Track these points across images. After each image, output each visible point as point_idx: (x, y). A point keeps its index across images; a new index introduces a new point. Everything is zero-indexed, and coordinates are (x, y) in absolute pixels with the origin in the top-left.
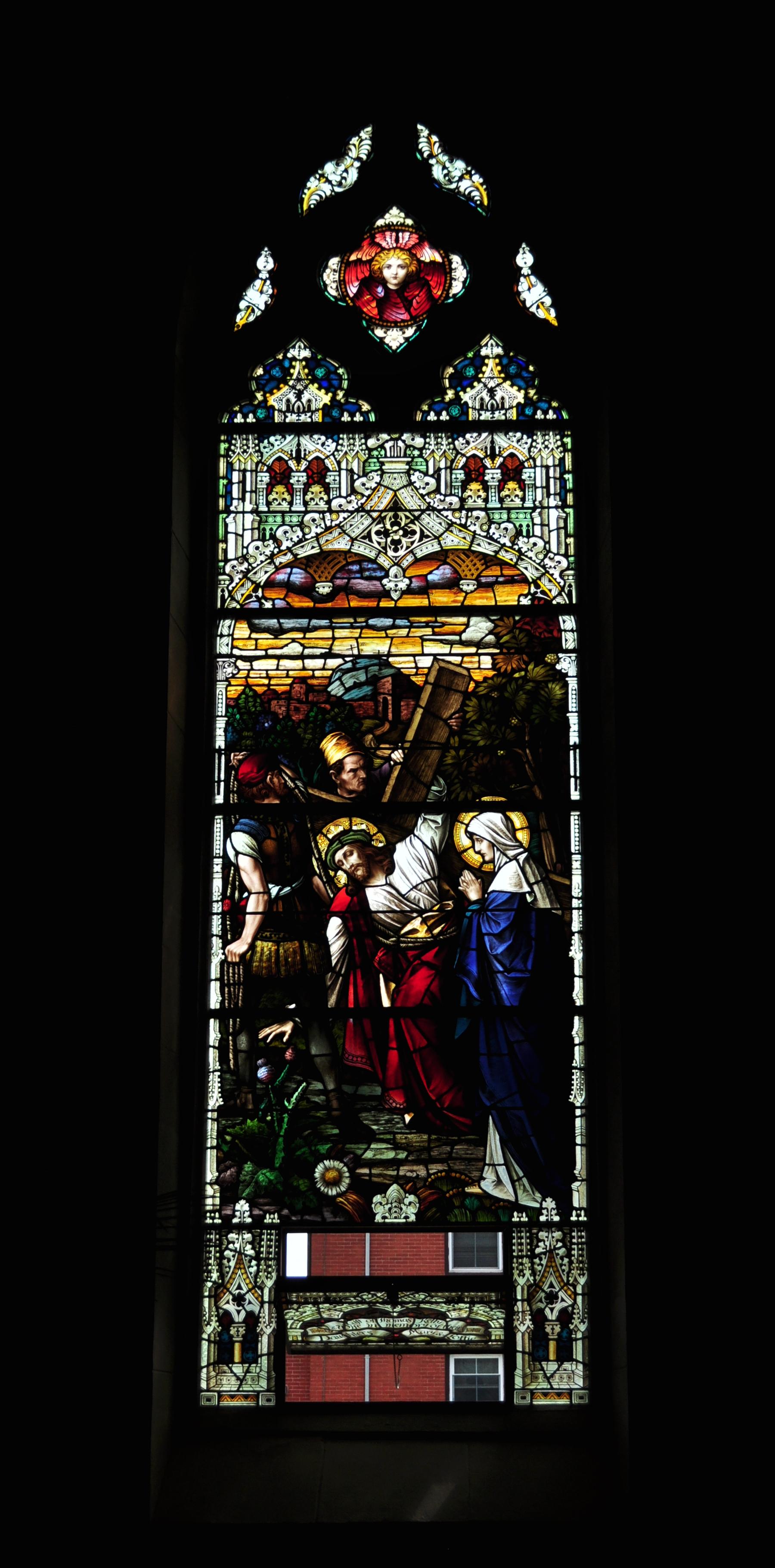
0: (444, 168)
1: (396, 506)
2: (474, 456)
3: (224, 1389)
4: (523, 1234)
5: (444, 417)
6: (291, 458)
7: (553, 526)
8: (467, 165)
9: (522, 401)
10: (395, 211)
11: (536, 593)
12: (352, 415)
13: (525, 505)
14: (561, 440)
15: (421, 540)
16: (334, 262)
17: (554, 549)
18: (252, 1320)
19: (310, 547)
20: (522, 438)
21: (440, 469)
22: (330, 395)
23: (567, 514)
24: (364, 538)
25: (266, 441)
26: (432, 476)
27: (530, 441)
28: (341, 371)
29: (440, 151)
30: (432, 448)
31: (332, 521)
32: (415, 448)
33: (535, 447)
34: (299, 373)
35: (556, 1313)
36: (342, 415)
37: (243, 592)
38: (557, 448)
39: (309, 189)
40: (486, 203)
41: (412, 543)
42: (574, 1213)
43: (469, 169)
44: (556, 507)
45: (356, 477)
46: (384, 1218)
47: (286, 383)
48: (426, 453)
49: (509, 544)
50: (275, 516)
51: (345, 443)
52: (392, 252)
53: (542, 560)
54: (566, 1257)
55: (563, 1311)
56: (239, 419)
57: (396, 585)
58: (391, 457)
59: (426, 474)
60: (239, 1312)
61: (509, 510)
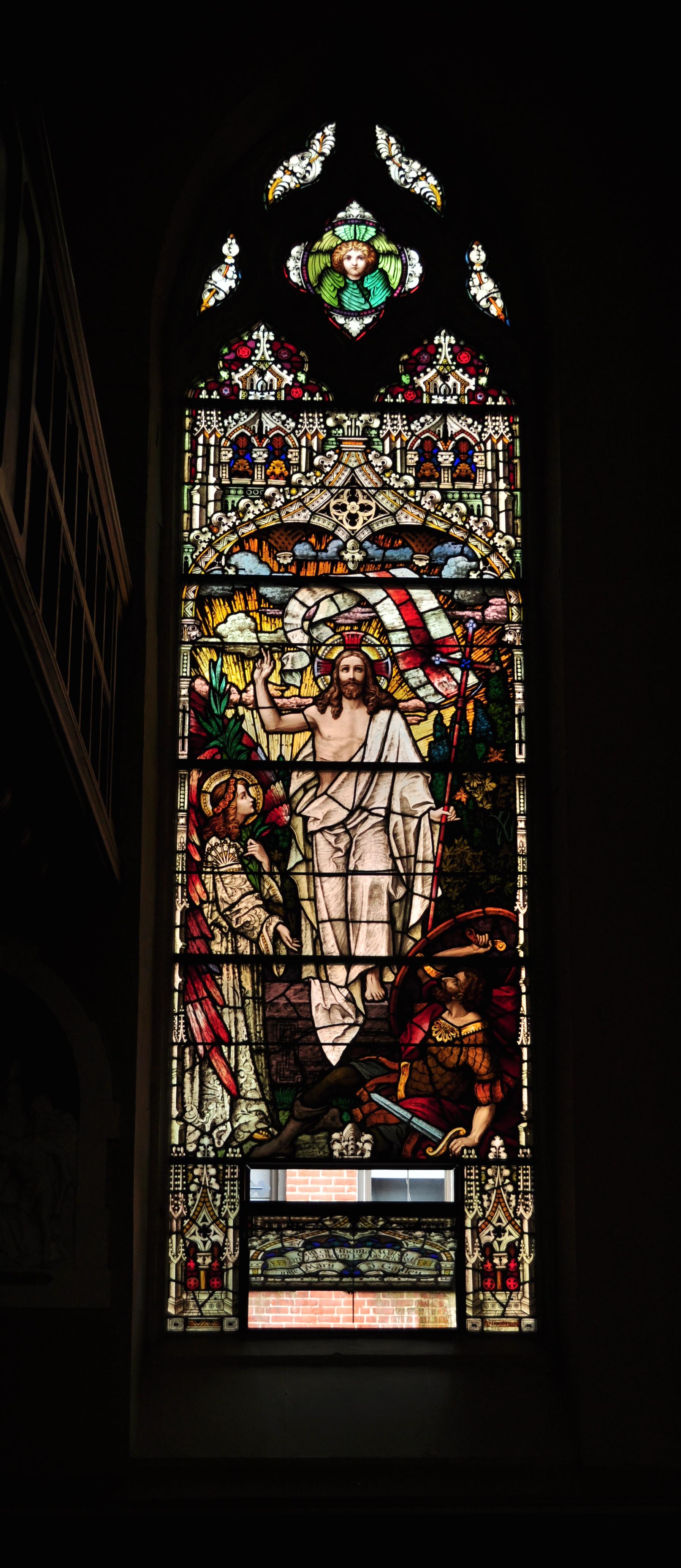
0: (401, 169)
1: (353, 485)
2: (428, 438)
3: (191, 1314)
4: (472, 1171)
5: (400, 399)
6: (255, 435)
7: (502, 507)
8: (422, 167)
9: (473, 388)
10: (355, 205)
11: (485, 569)
12: (312, 395)
13: (476, 487)
14: (510, 426)
15: (376, 515)
16: (296, 251)
17: (503, 527)
18: (217, 1250)
19: (271, 519)
20: (473, 424)
21: (396, 449)
22: (292, 376)
23: (515, 497)
24: (323, 511)
25: (230, 417)
26: (388, 455)
27: (480, 427)
28: (302, 354)
29: (396, 152)
30: (389, 428)
31: (291, 495)
32: (372, 429)
33: (486, 432)
34: (263, 354)
35: (503, 1247)
36: (303, 396)
37: (207, 559)
38: (507, 434)
39: (275, 180)
40: (439, 203)
41: (369, 517)
42: (521, 1151)
43: (424, 170)
44: (505, 490)
45: (315, 454)
46: (341, 1154)
47: (250, 363)
48: (383, 434)
49: (460, 523)
50: (237, 490)
51: (306, 422)
52: (350, 244)
53: (492, 538)
54: (513, 1193)
55: (511, 1245)
56: (204, 395)
57: (353, 557)
58: (348, 436)
59: (382, 454)
60: (205, 1243)
61: (461, 490)
